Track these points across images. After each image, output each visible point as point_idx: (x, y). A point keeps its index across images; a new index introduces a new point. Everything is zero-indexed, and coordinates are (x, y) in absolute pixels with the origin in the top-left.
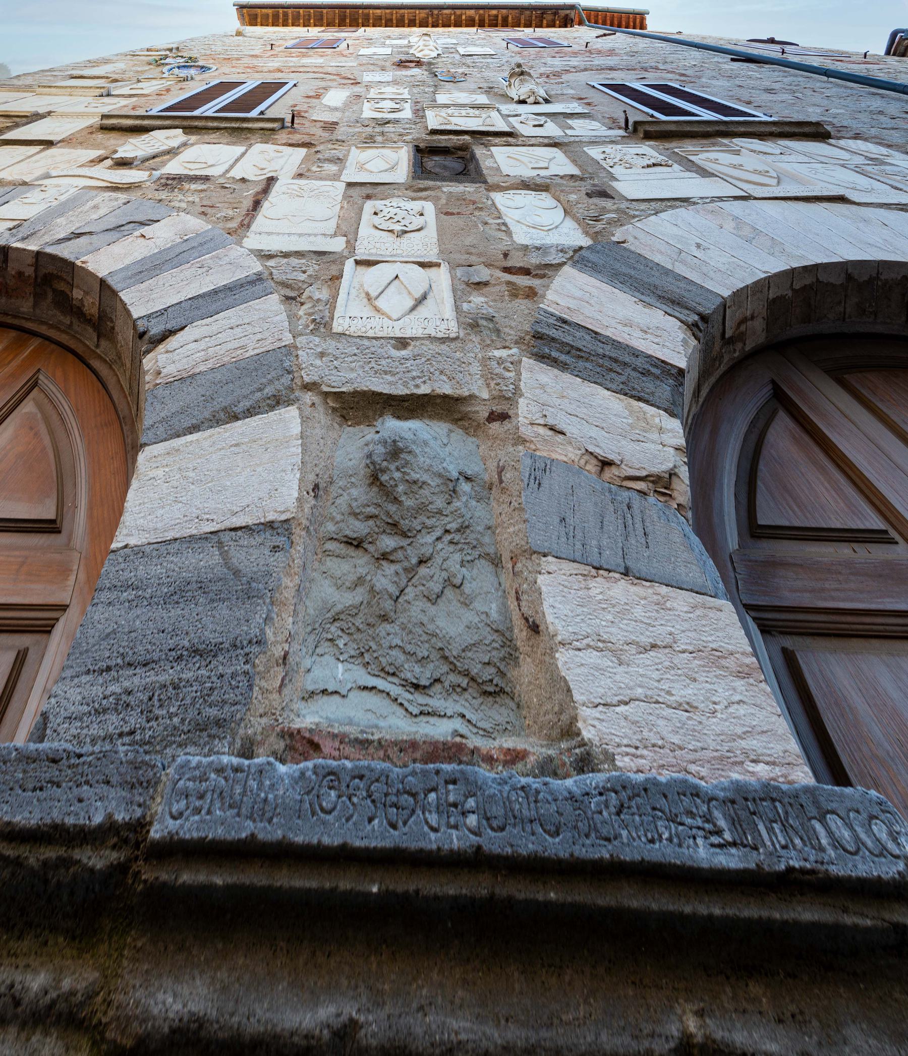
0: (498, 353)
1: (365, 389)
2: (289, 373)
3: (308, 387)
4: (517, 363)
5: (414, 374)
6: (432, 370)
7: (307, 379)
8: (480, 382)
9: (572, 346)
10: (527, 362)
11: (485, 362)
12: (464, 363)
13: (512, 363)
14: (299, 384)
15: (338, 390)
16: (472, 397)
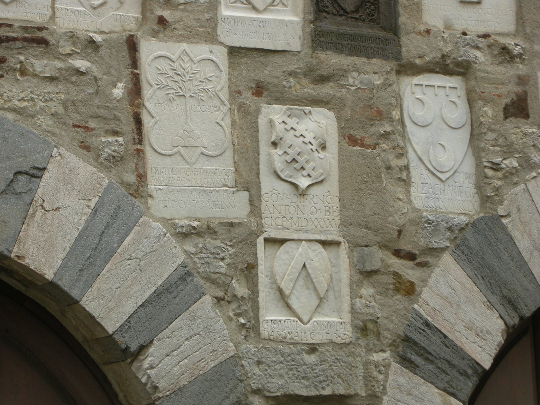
0: (377, 357)
1: (292, 393)
2: (241, 381)
3: (257, 392)
4: (387, 366)
5: (322, 378)
6: (333, 375)
7: (254, 387)
8: (362, 382)
9: (426, 350)
10: (395, 366)
11: (366, 364)
12: (354, 367)
13: (384, 366)
14: (249, 390)
15: (275, 395)
16: (356, 395)
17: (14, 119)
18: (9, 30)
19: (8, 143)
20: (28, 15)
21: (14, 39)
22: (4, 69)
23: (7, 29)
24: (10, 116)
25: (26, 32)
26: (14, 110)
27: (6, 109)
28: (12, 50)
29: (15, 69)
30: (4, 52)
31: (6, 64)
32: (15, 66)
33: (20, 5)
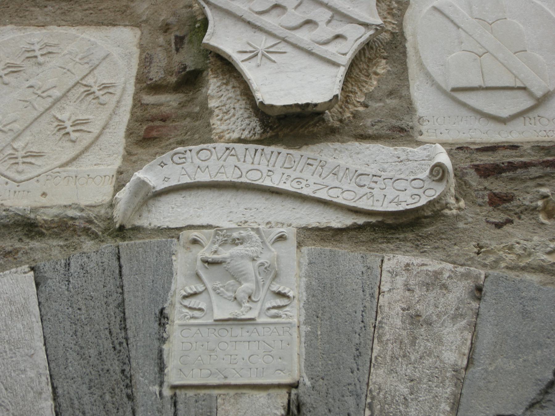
17: (541, 282)
18: (514, 154)
19: (533, 320)
20: (550, 134)
21: (525, 165)
22: (511, 210)
23: (508, 152)
24: (535, 278)
25: (548, 154)
26: (541, 269)
27: (523, 269)
28: (524, 181)
29: (535, 209)
30: (509, 187)
31: (515, 203)
32: (534, 204)
33: (533, 121)
